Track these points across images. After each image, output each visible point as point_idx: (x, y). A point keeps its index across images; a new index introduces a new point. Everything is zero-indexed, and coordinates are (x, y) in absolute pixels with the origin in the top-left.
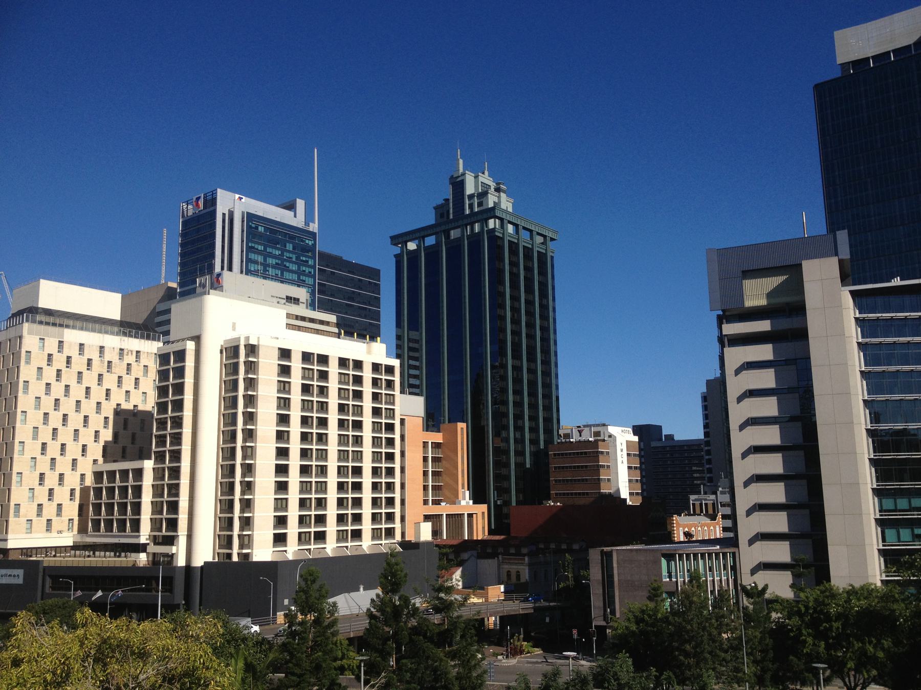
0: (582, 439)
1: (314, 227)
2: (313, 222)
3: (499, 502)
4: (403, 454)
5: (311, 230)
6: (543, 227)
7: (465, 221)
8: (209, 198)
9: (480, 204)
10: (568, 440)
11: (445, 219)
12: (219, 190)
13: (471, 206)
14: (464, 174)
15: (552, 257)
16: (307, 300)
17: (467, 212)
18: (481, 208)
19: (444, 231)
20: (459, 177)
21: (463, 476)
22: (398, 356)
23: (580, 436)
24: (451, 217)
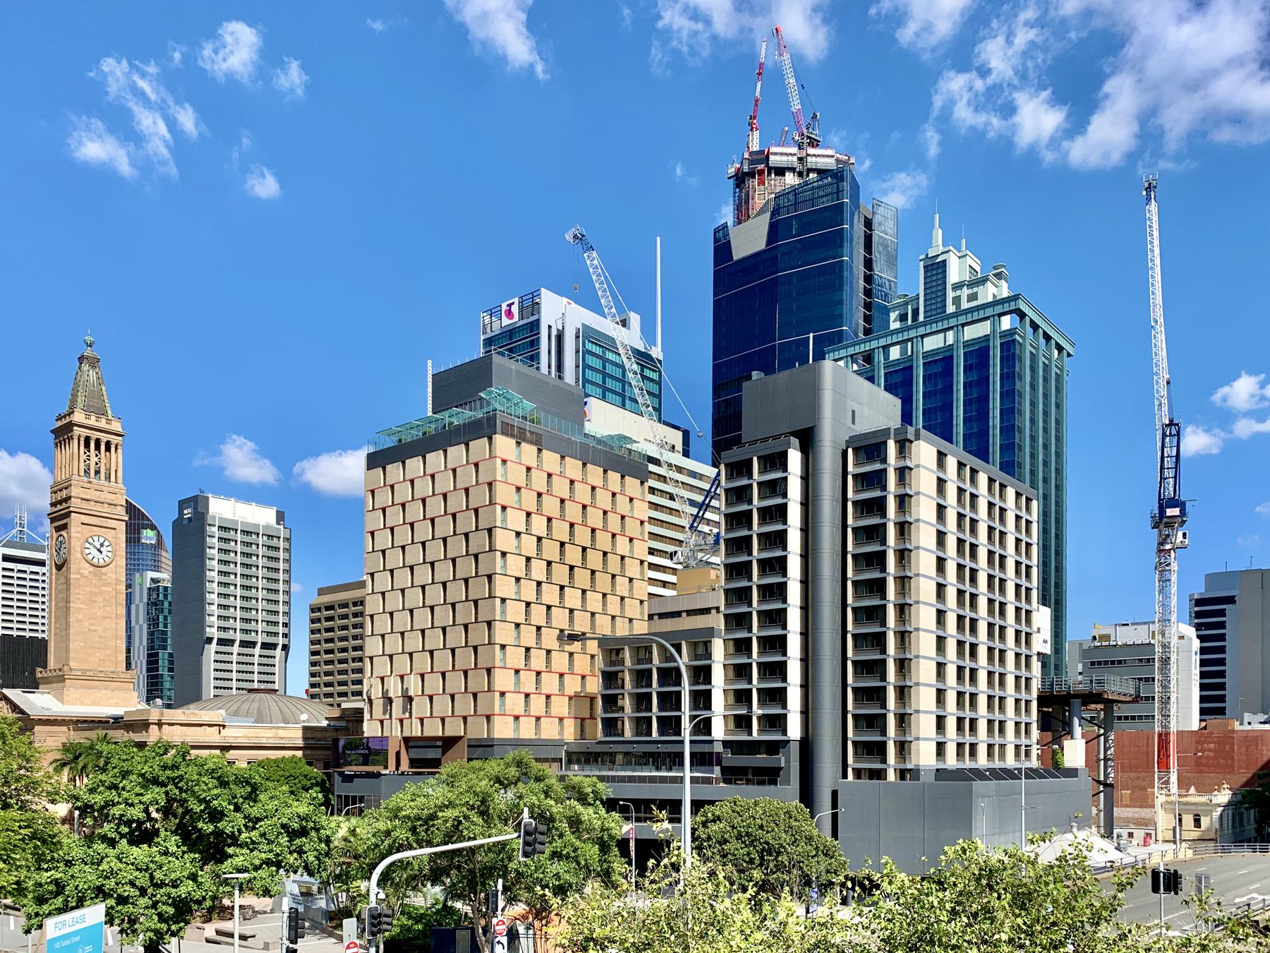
11: (910, 322)
12: (543, 290)
13: (957, 300)
17: (951, 309)
18: (974, 304)
24: (921, 318)
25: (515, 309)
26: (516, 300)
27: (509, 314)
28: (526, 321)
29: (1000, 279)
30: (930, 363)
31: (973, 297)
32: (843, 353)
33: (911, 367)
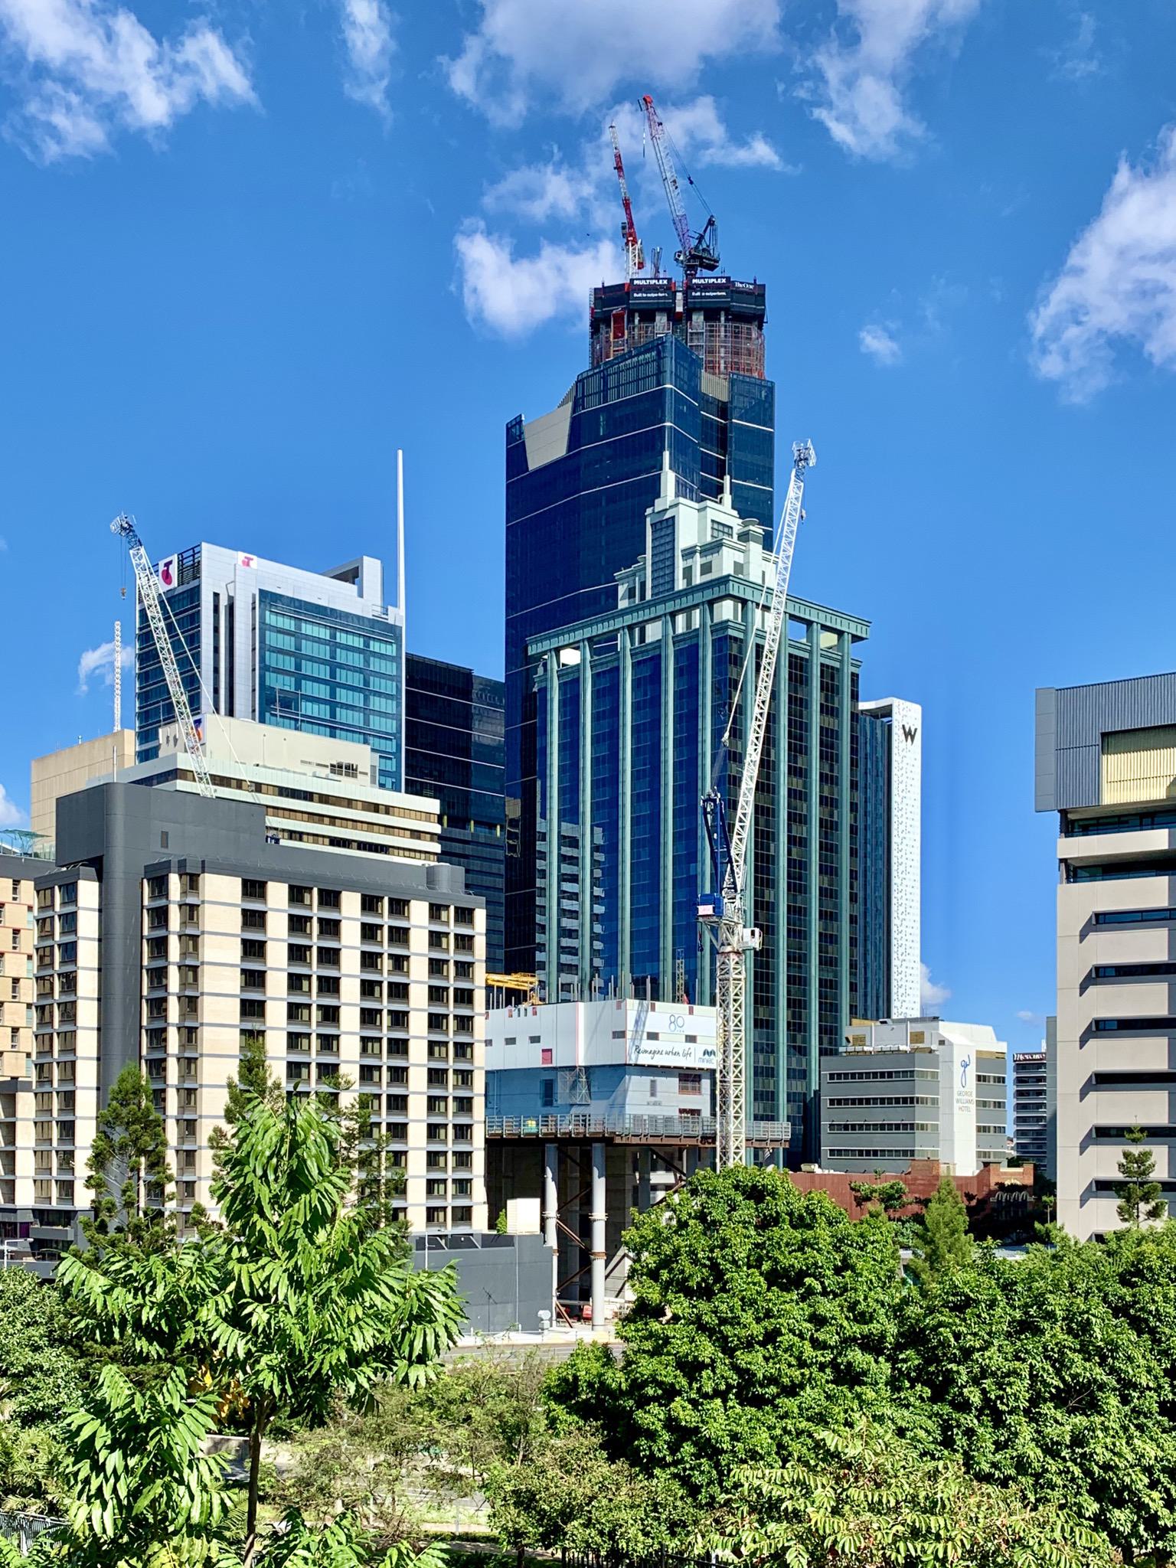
1: (397, 616)
2: (395, 605)
5: (391, 621)
6: (836, 613)
7: (670, 607)
8: (188, 562)
9: (706, 568)
11: (637, 601)
12: (204, 545)
13: (688, 572)
15: (855, 677)
16: (373, 767)
17: (680, 584)
18: (708, 577)
19: (631, 628)
20: (666, 510)
24: (648, 597)
25: (174, 570)
26: (175, 558)
27: (167, 577)
28: (186, 587)
29: (747, 541)
30: (639, 663)
31: (706, 568)
32: (579, 635)
33: (617, 668)
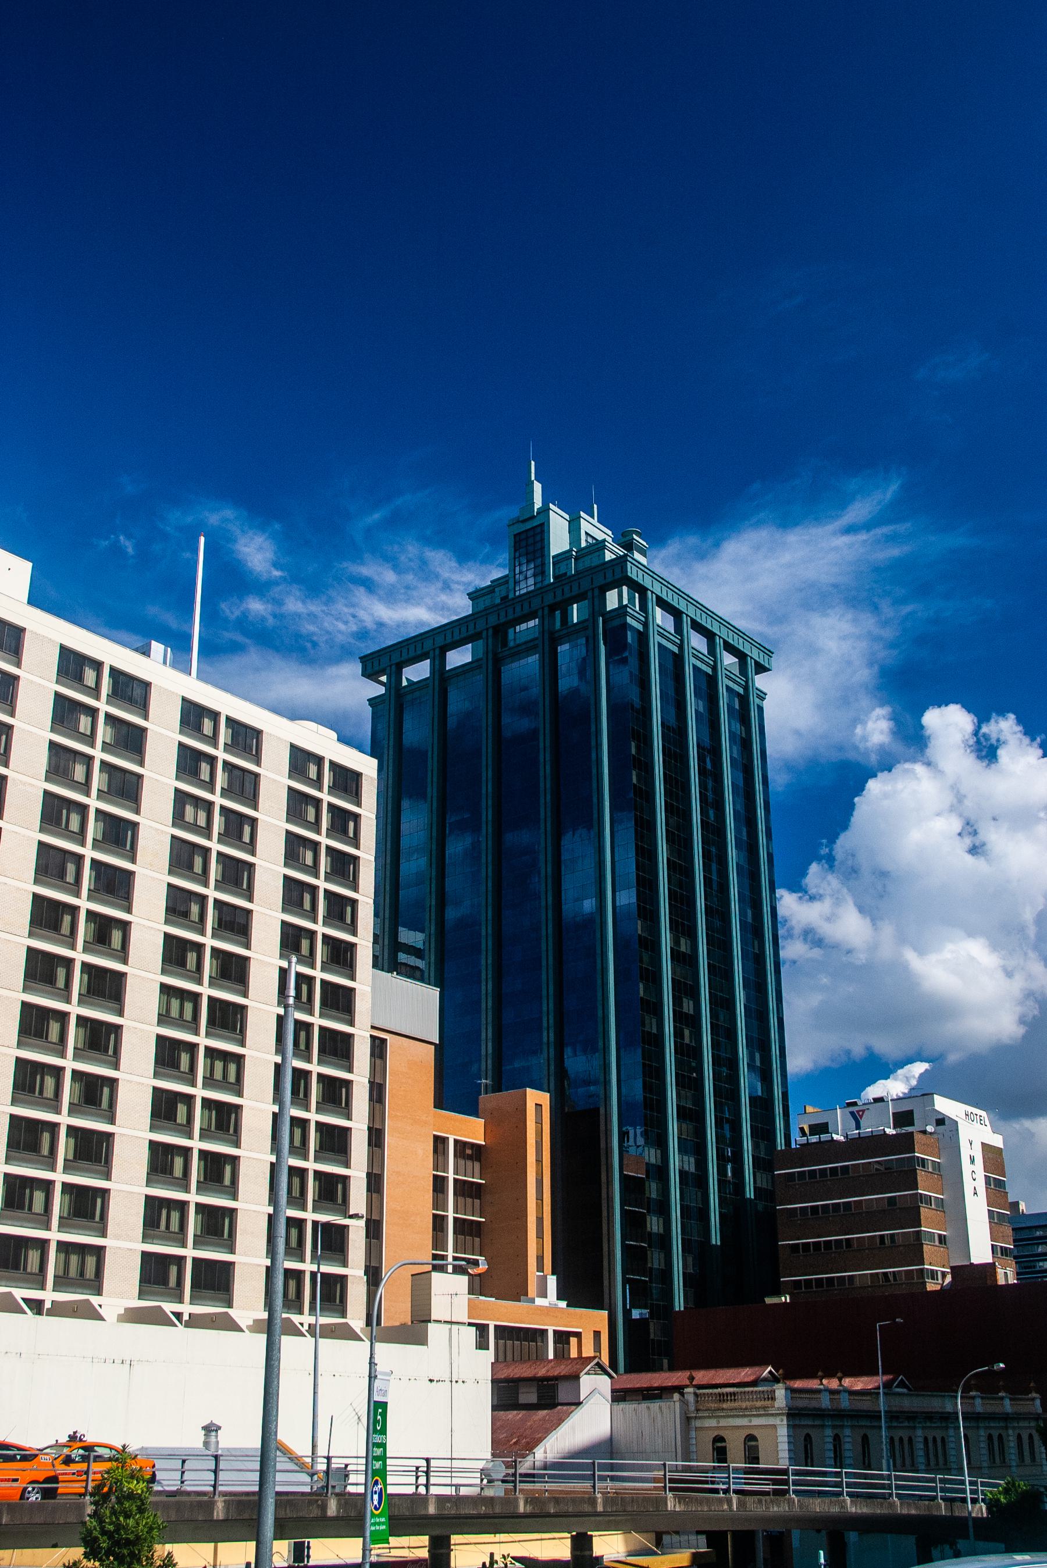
0: (867, 1130)
3: (636, 1314)
4: (376, 1137)
10: (824, 1137)
14: (545, 510)
15: (761, 709)
21: (540, 1235)
22: (374, 752)
23: (858, 1127)
